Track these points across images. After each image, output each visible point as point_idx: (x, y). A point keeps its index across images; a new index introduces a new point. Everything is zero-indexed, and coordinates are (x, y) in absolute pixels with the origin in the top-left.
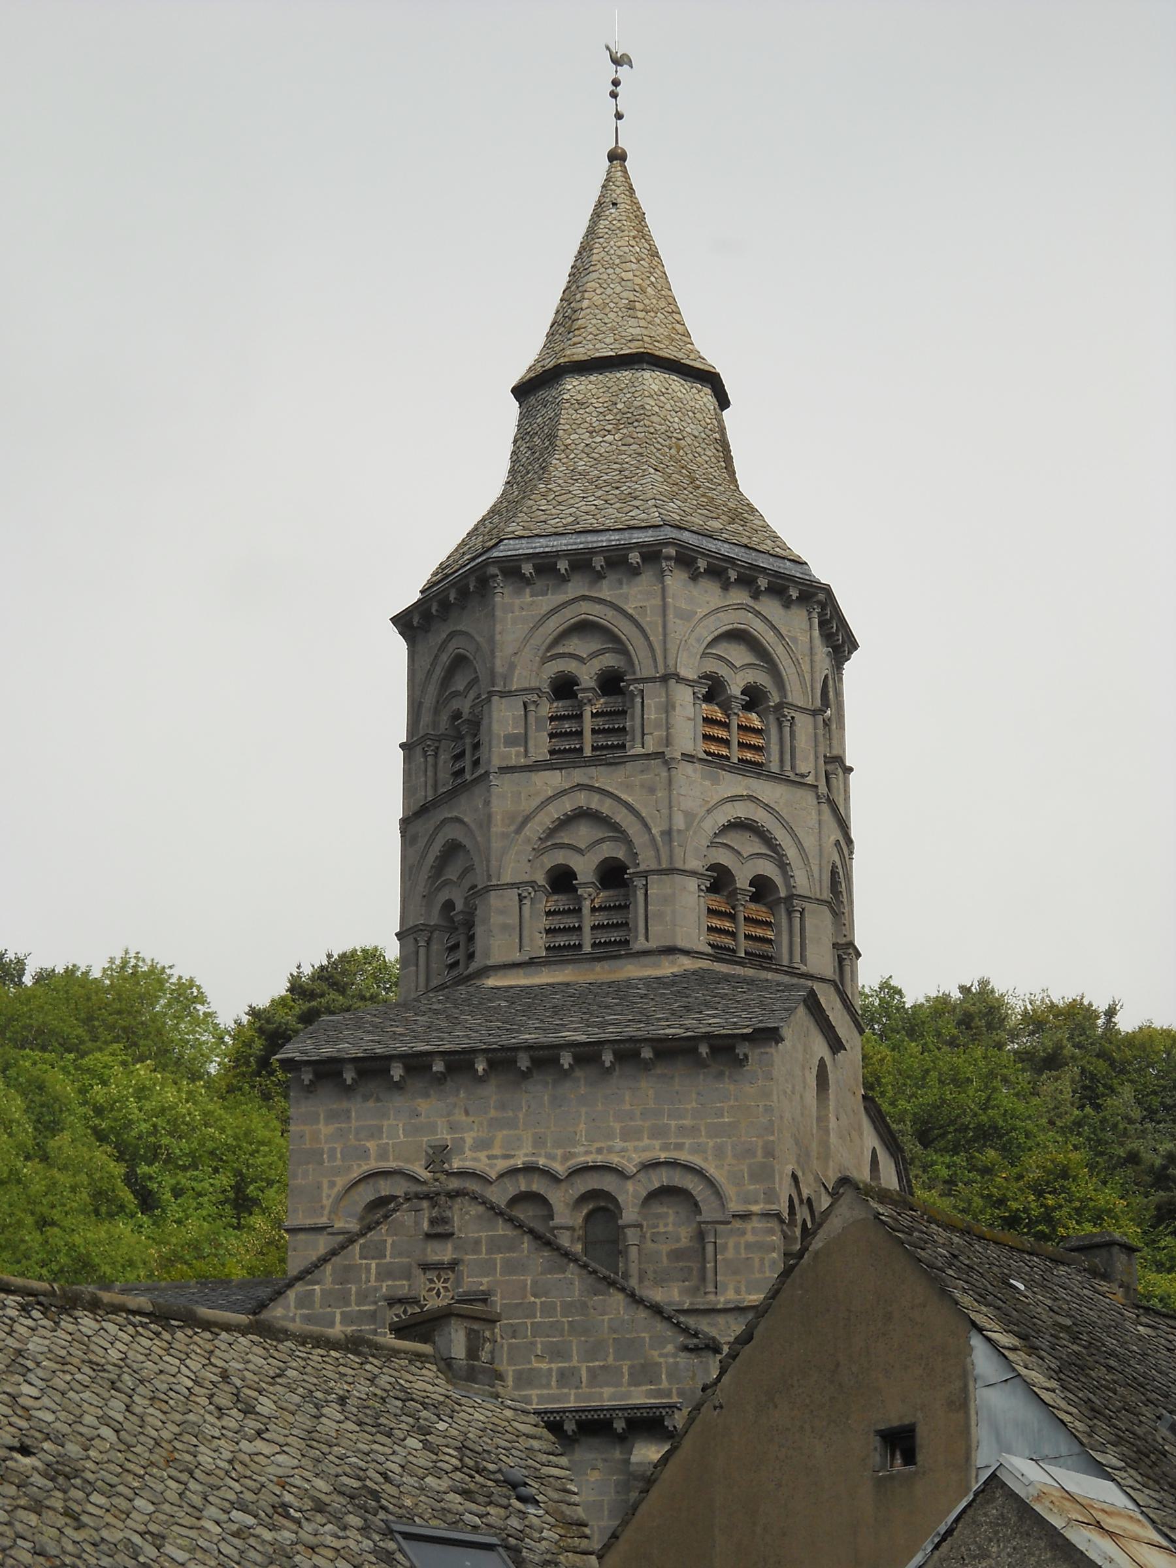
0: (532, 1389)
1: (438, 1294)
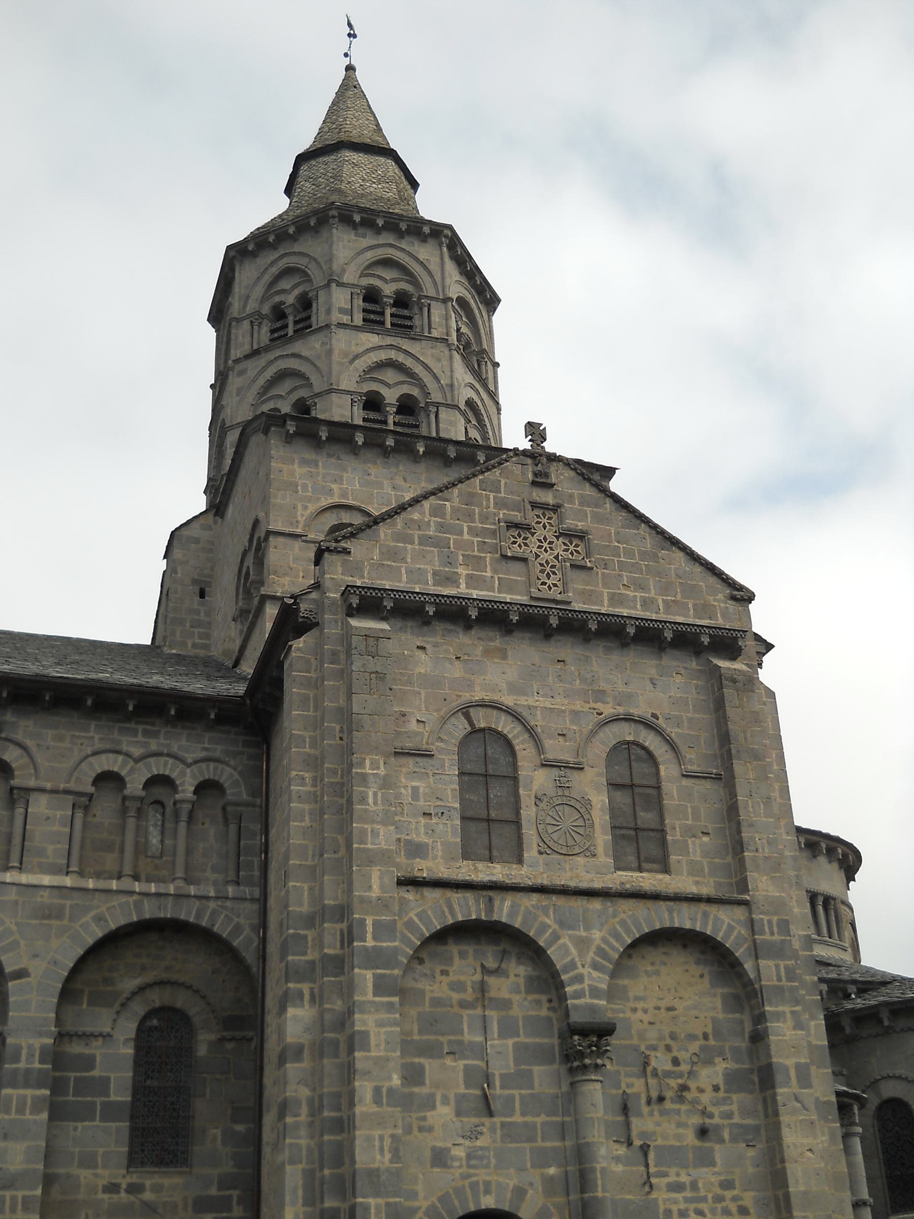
0: (623, 608)
1: (545, 527)
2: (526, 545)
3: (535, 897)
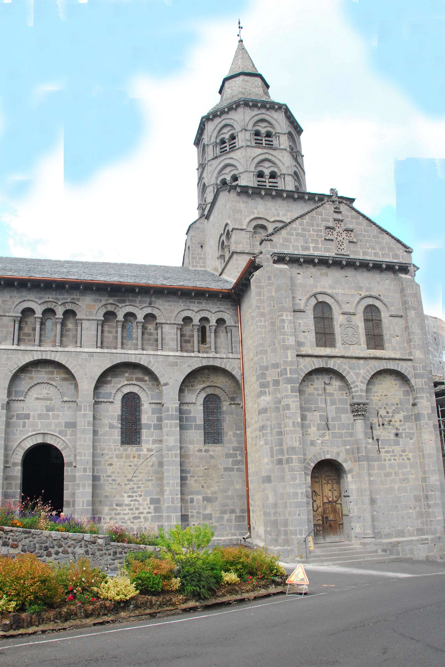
2: (333, 234)
3: (341, 359)
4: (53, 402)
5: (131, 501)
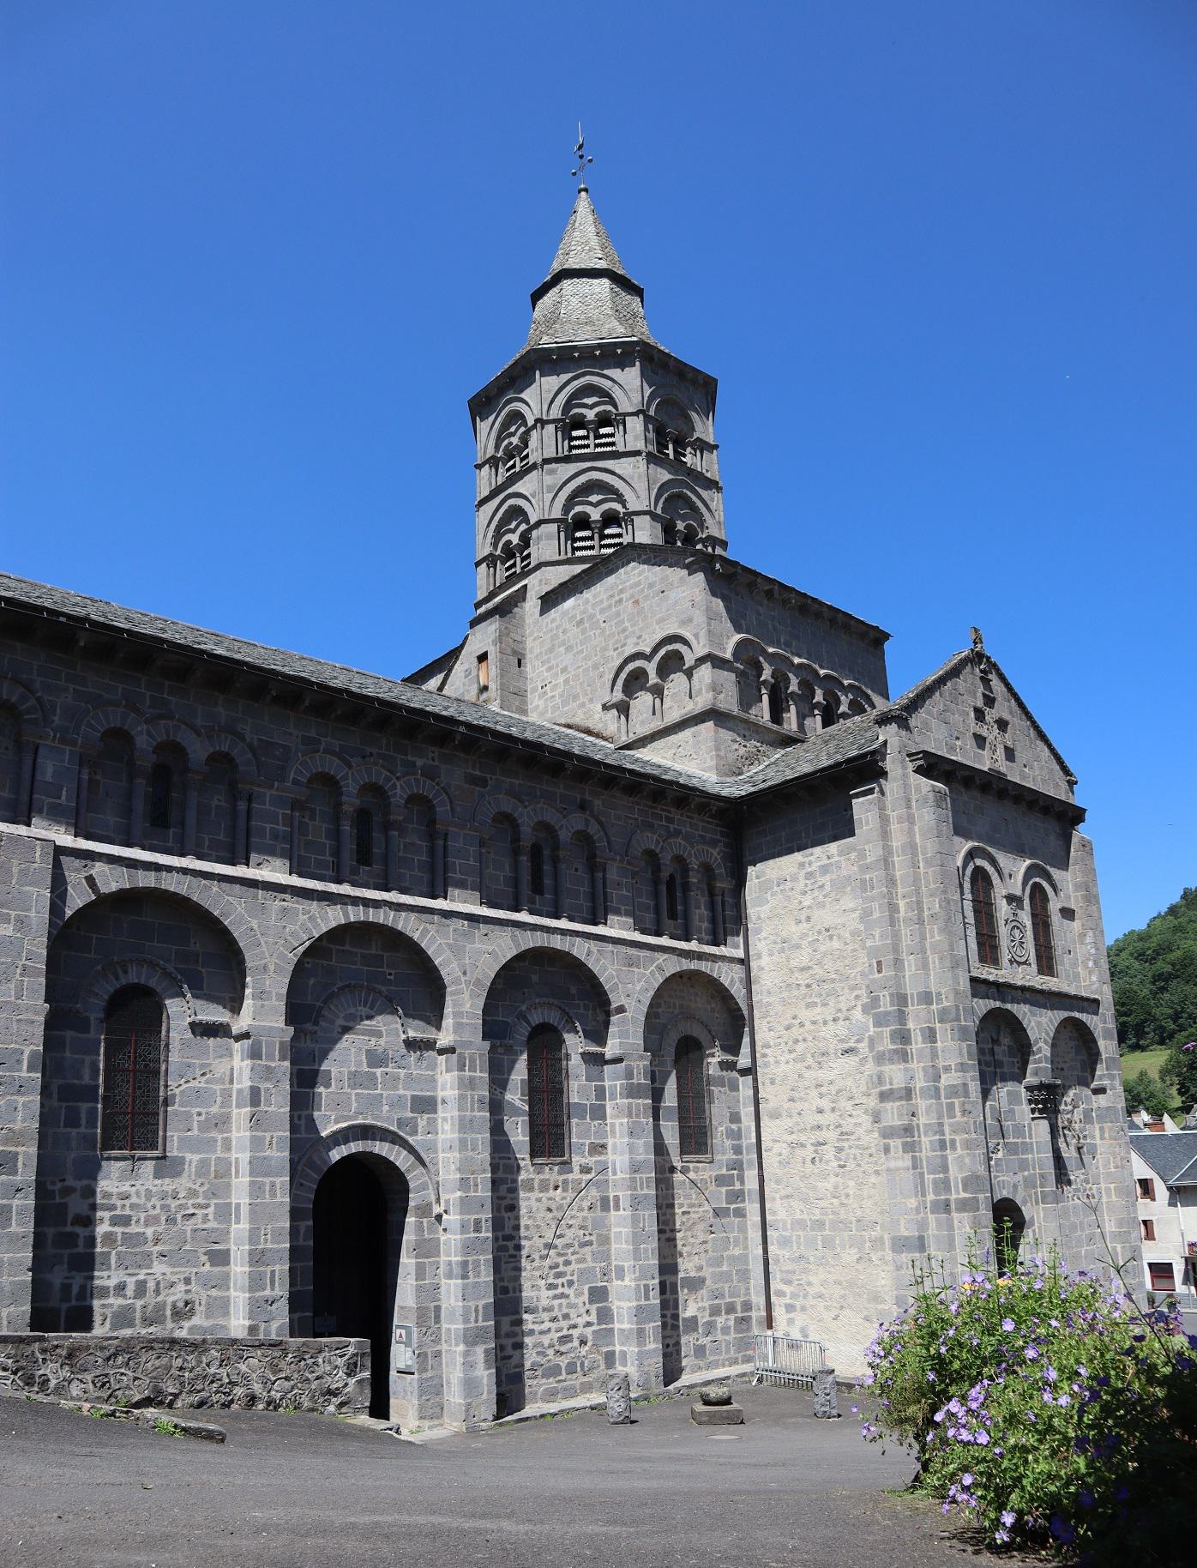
4: (382, 1042)
5: (556, 1297)
